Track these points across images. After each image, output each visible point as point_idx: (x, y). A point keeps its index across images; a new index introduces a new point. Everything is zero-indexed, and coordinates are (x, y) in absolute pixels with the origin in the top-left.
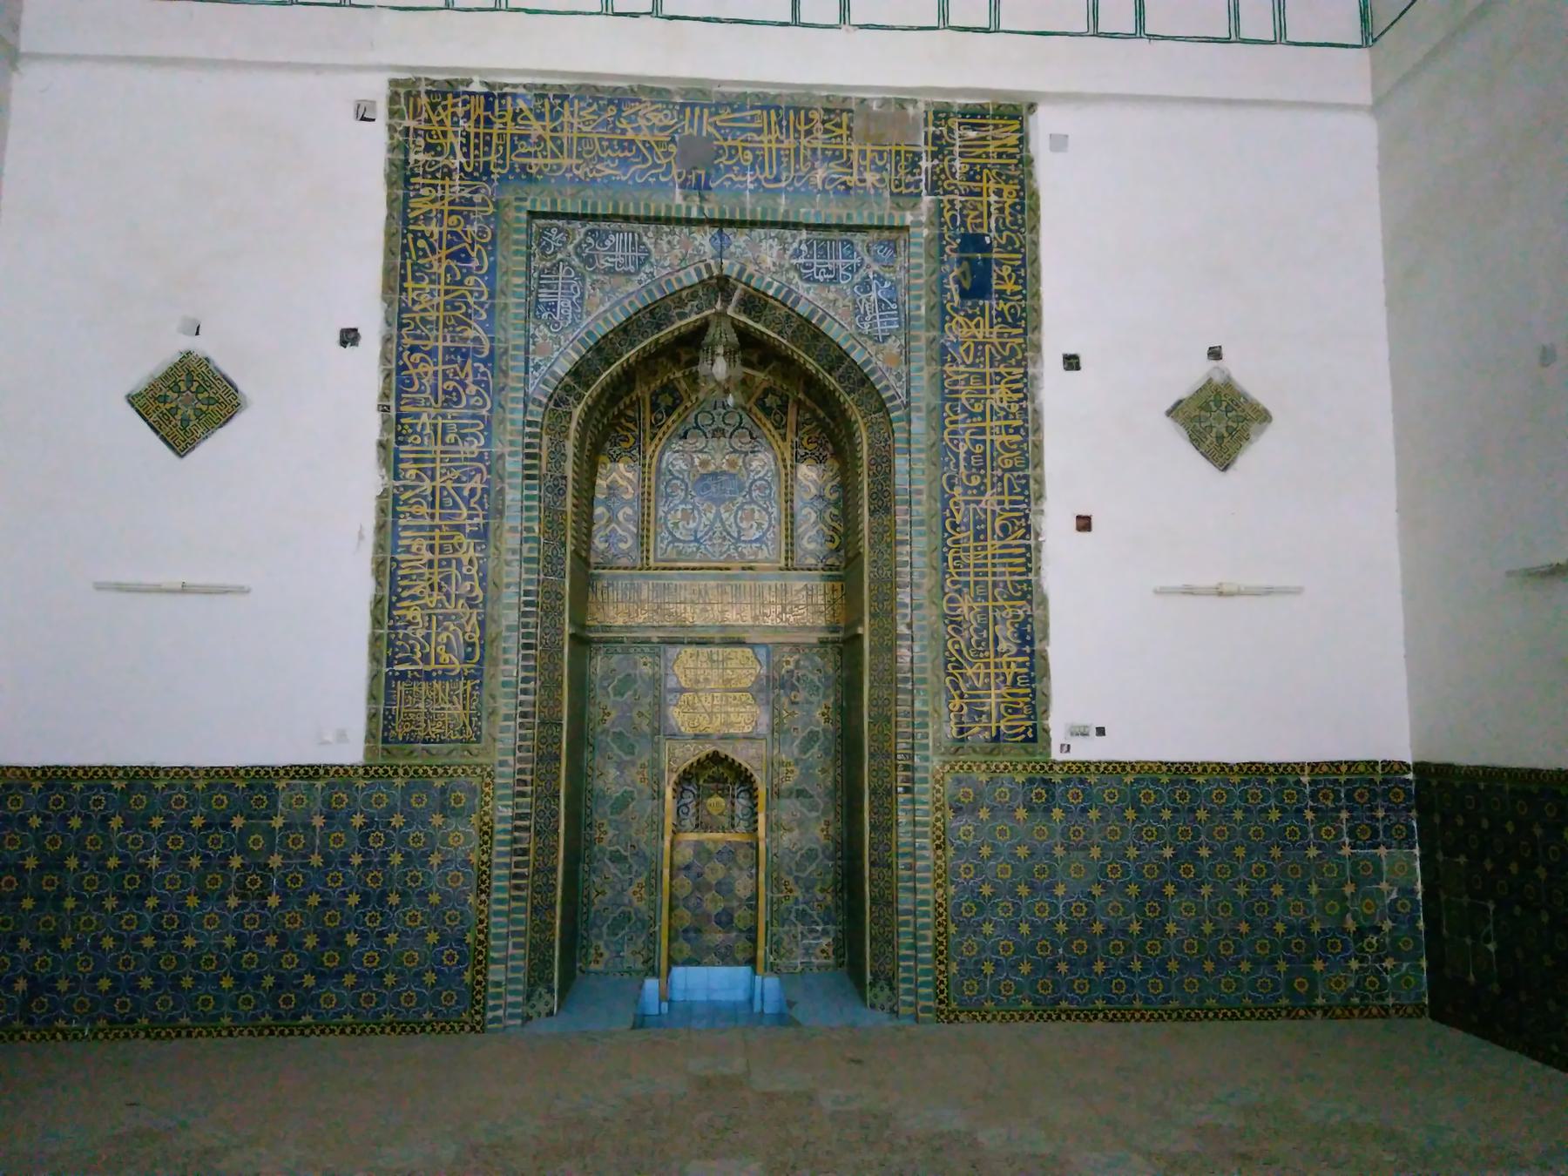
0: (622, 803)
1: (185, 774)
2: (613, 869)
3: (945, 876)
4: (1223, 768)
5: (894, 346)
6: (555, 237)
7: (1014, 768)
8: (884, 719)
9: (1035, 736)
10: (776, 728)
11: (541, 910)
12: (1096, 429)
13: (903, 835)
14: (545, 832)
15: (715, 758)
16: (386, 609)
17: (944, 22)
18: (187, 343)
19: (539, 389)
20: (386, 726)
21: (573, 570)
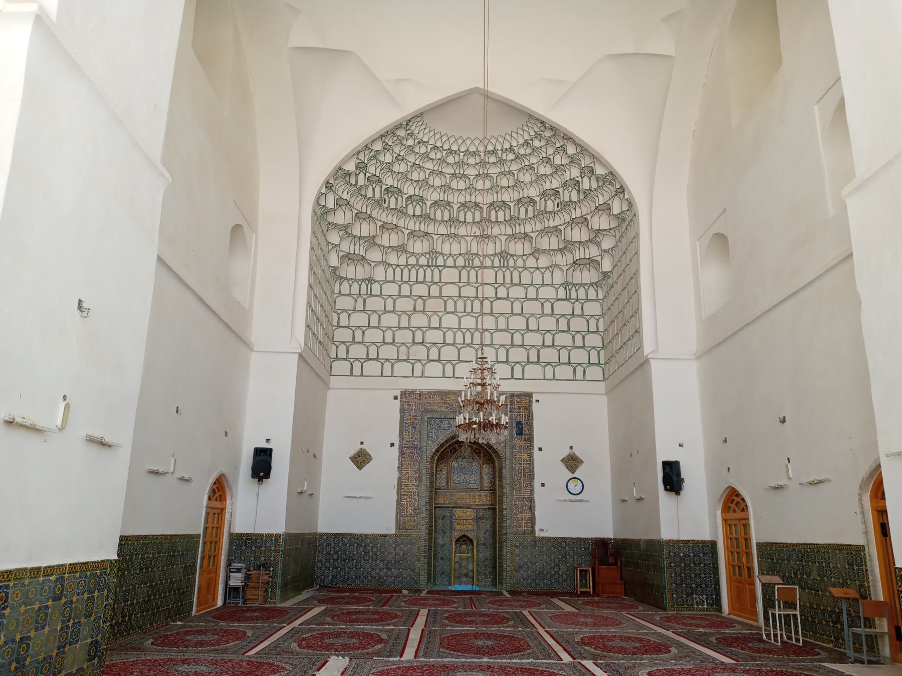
0: (443, 546)
1: (361, 535)
2: (441, 561)
3: (513, 561)
4: (572, 539)
5: (503, 445)
6: (432, 423)
7: (530, 538)
8: (501, 527)
9: (533, 531)
10: (478, 529)
11: (429, 566)
12: (547, 465)
13: (504, 553)
14: (430, 549)
15: (464, 536)
16: (399, 502)
17: (512, 378)
18: (362, 446)
19: (430, 454)
20: (399, 525)
21: (434, 491)
